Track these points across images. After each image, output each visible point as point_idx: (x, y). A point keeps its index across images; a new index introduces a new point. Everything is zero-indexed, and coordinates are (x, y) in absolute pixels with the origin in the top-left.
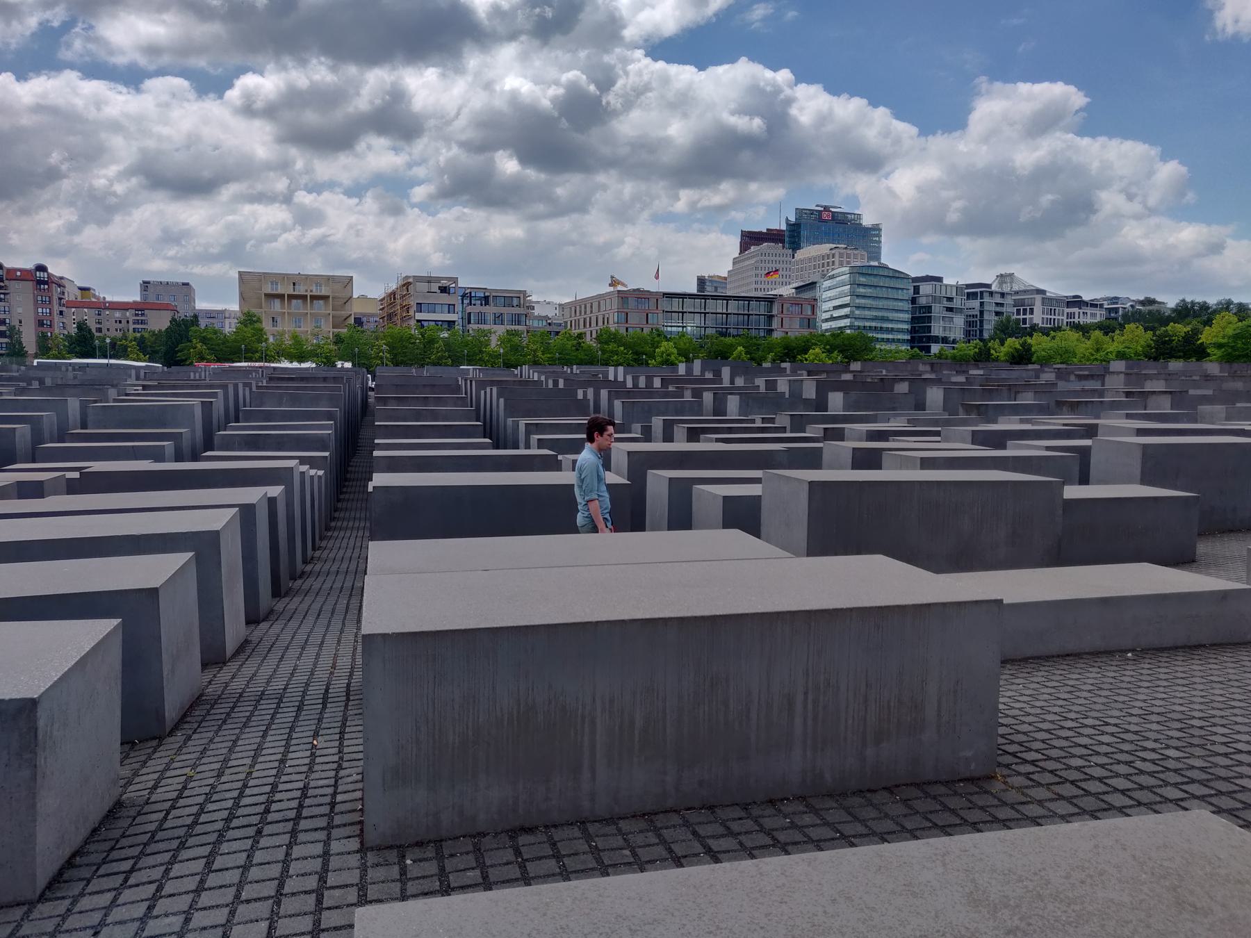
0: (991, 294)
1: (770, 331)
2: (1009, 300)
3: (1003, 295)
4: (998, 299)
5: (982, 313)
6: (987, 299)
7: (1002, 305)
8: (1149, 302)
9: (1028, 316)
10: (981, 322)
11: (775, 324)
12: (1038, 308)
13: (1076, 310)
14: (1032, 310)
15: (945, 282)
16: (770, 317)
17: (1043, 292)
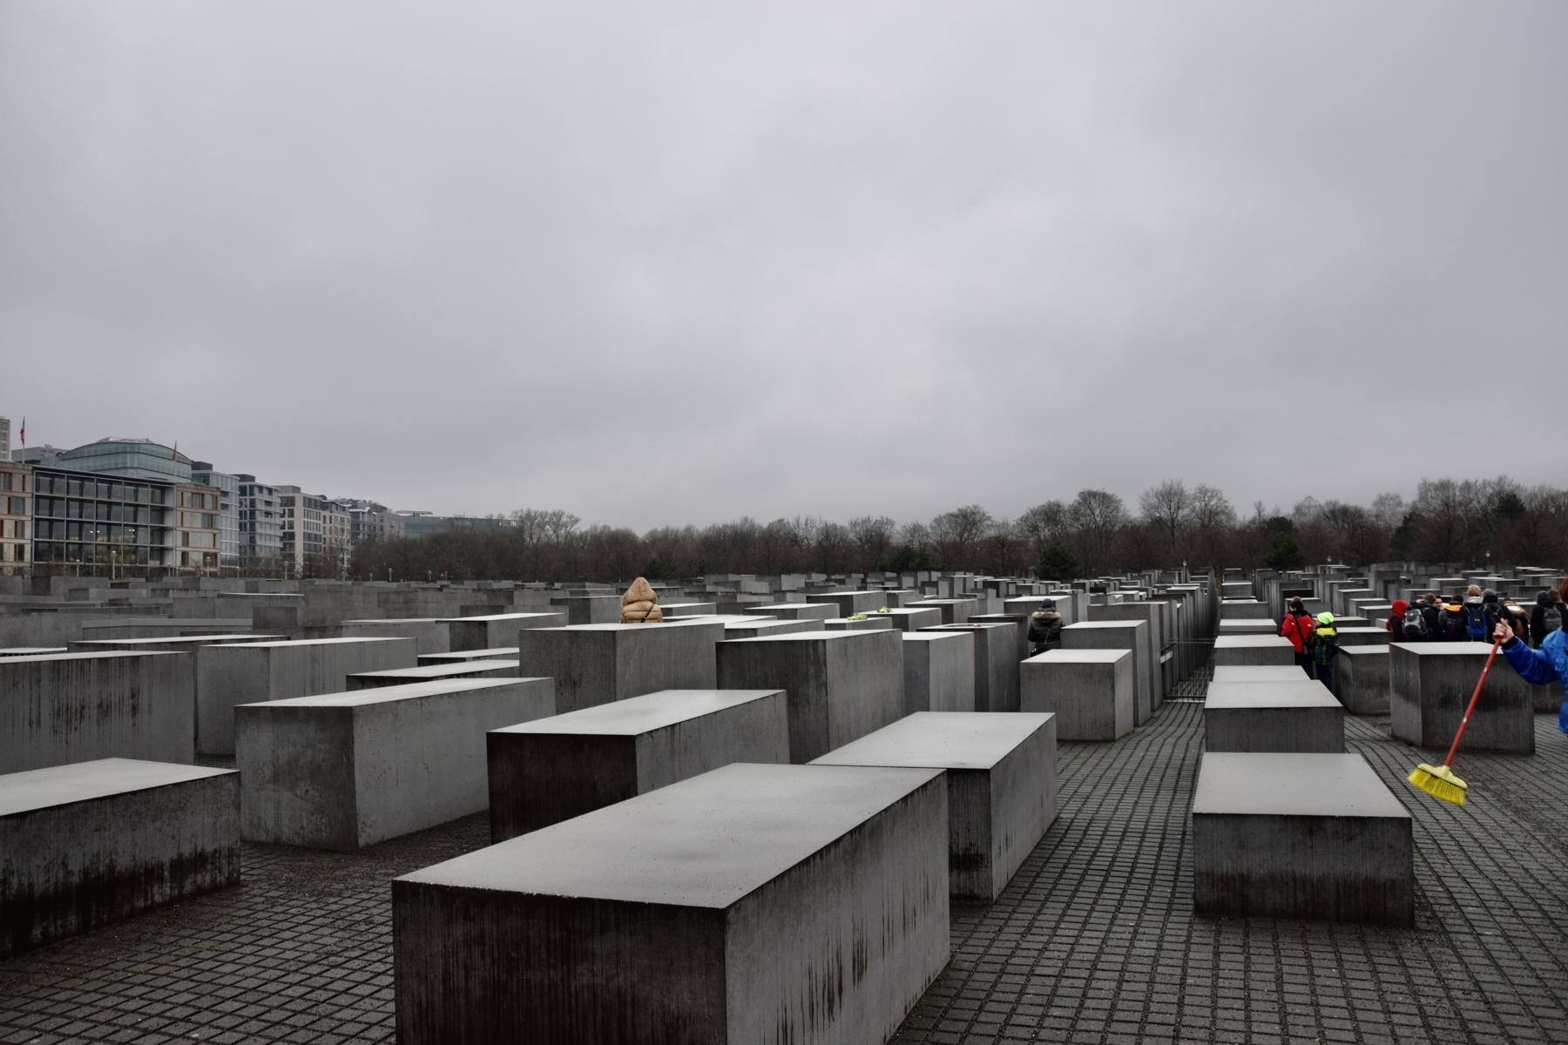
0: (261, 488)
1: (161, 532)
2: (275, 499)
3: (270, 491)
4: (266, 496)
5: (253, 513)
6: (257, 496)
7: (268, 503)
8: (376, 508)
9: (287, 519)
10: (253, 525)
11: (170, 521)
12: (299, 508)
13: (327, 513)
14: (291, 514)
15: (215, 469)
16: (161, 512)
17: (297, 490)
